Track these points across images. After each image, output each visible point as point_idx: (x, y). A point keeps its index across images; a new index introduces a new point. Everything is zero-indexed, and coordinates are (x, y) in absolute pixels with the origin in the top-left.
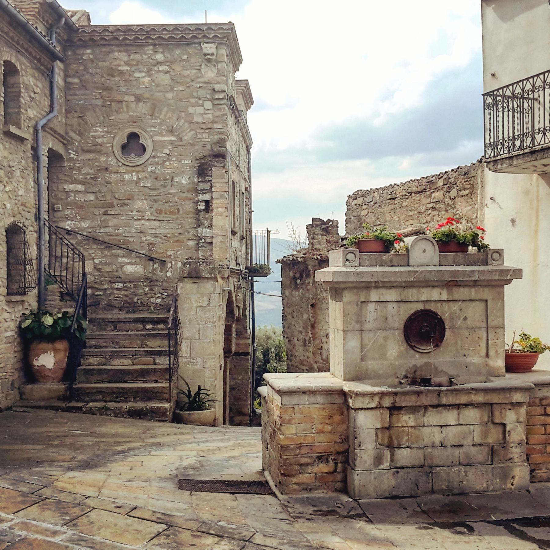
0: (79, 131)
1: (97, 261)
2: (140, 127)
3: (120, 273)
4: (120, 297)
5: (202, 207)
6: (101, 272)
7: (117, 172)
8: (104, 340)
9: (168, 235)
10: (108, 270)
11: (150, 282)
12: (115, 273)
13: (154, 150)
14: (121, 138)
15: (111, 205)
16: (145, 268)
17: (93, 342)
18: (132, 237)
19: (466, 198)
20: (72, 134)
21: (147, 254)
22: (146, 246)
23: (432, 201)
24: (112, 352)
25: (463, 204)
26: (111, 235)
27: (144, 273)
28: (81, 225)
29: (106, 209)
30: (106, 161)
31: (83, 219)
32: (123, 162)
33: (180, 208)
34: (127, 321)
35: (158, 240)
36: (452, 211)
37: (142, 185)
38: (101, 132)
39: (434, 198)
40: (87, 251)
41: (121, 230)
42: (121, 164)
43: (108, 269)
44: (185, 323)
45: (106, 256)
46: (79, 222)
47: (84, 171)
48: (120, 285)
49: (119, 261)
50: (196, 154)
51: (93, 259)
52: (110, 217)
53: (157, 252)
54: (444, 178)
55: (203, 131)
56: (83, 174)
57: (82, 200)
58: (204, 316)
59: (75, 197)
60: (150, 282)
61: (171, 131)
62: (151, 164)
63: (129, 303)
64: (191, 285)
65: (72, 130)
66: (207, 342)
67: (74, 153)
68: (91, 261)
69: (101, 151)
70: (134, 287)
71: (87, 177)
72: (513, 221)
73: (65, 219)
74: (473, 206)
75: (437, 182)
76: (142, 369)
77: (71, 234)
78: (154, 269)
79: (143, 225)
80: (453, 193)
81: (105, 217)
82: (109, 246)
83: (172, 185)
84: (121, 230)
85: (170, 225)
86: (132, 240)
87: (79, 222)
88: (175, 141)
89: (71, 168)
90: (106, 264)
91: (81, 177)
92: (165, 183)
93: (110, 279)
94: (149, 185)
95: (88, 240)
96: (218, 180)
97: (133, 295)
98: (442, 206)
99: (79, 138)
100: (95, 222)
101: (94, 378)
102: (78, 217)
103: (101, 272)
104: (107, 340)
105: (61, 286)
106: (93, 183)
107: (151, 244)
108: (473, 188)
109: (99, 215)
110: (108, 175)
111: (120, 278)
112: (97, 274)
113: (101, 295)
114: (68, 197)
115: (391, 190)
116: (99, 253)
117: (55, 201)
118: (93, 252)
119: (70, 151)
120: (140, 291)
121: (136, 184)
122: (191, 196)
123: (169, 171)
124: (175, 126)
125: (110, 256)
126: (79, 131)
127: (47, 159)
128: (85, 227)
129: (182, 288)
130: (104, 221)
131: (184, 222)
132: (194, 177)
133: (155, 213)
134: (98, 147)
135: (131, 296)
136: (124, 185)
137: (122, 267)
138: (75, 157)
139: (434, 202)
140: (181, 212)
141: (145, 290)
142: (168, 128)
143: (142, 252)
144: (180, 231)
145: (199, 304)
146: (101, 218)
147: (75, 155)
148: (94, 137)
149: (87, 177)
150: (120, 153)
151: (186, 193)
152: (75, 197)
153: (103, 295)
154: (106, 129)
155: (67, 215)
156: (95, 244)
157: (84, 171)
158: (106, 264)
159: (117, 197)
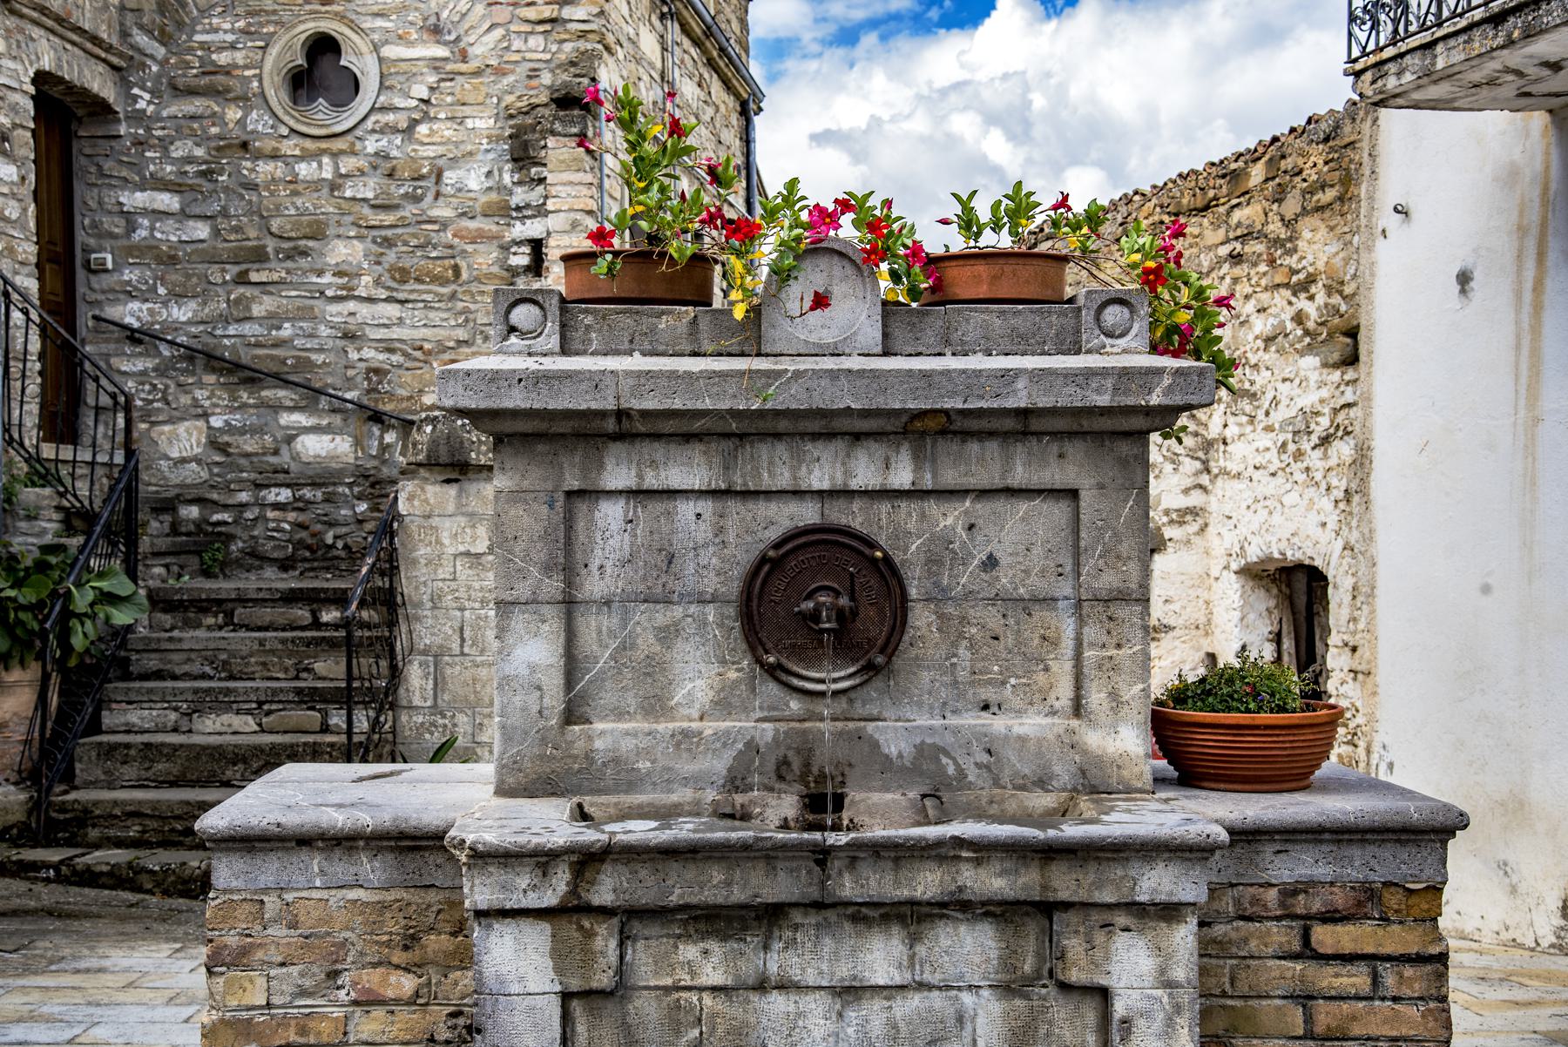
0: (162, 31)
1: (217, 422)
2: (341, 17)
3: (284, 459)
4: (283, 530)
5: (521, 259)
6: (228, 455)
7: (275, 156)
8: (184, 656)
9: (427, 346)
10: (249, 449)
11: (373, 486)
12: (273, 460)
13: (382, 87)
14: (286, 50)
15: (259, 256)
16: (358, 443)
17: (152, 663)
18: (321, 350)
19: (1328, 214)
20: (141, 39)
21: (365, 402)
22: (359, 379)
23: (1231, 235)
24: (196, 691)
25: (1319, 236)
26: (258, 345)
27: (357, 458)
28: (169, 315)
29: (244, 267)
30: (241, 122)
31: (178, 296)
32: (292, 123)
33: (463, 264)
34: (265, 600)
35: (396, 358)
36: (1287, 261)
37: (348, 194)
38: (226, 32)
39: (1239, 225)
40: (187, 393)
41: (287, 331)
42: (285, 131)
43: (250, 445)
44: (419, 605)
45: (244, 406)
46: (165, 304)
47: (178, 151)
48: (285, 495)
49: (283, 422)
50: (509, 99)
51: (205, 416)
52: (256, 291)
53: (391, 395)
54: (1267, 157)
55: (528, 28)
56: (174, 161)
57: (174, 239)
58: (477, 585)
59: (152, 229)
60: (373, 486)
61: (436, 31)
62: (373, 131)
63: (309, 548)
64: (437, 488)
65: (141, 27)
66: (483, 664)
67: (147, 96)
68: (201, 423)
69: (228, 90)
70: (326, 500)
71: (188, 168)
72: (1464, 279)
73: (122, 296)
74: (1348, 237)
75: (1248, 175)
76: (273, 746)
77: (140, 342)
78: (384, 448)
79: (352, 314)
80: (1291, 206)
81: (241, 290)
82: (243, 374)
83: (438, 195)
84: (287, 331)
85: (432, 315)
86: (319, 358)
87: (165, 304)
88: (445, 59)
89: (139, 143)
90: (242, 431)
91: (169, 168)
92: (415, 188)
93: (253, 476)
94: (370, 195)
95: (191, 359)
96: (566, 176)
97: (325, 523)
98: (1259, 247)
99: (163, 50)
100: (213, 305)
101: (130, 772)
102: (162, 291)
103: (228, 455)
104: (193, 656)
105: (61, 489)
106: (207, 186)
107: (377, 371)
108: (1348, 180)
109: (225, 282)
110: (248, 164)
111: (287, 472)
112: (218, 459)
113: (225, 523)
114: (131, 227)
115: (1123, 210)
116: (223, 398)
117: (92, 242)
118: (206, 393)
119: (136, 91)
120: (343, 512)
121: (332, 190)
122: (494, 228)
123: (430, 152)
124: (445, 14)
125: (255, 406)
126: (162, 31)
127: (30, 105)
128: (183, 319)
129: (410, 498)
130: (238, 301)
131: (472, 307)
132: (500, 170)
133: (386, 278)
134: (220, 78)
135: (319, 527)
136: (295, 193)
137: (290, 440)
138: (151, 108)
139: (1237, 238)
140: (465, 276)
141: (358, 510)
142: (425, 19)
143: (348, 396)
144: (462, 334)
145: (462, 548)
146: (229, 293)
147: (149, 103)
148: (205, 46)
149: (188, 168)
150: (285, 96)
151: (479, 218)
152: (152, 229)
153: (235, 522)
154: (241, 24)
155: (129, 283)
156: (213, 370)
157: (178, 151)
158: (242, 431)
159: (273, 230)
